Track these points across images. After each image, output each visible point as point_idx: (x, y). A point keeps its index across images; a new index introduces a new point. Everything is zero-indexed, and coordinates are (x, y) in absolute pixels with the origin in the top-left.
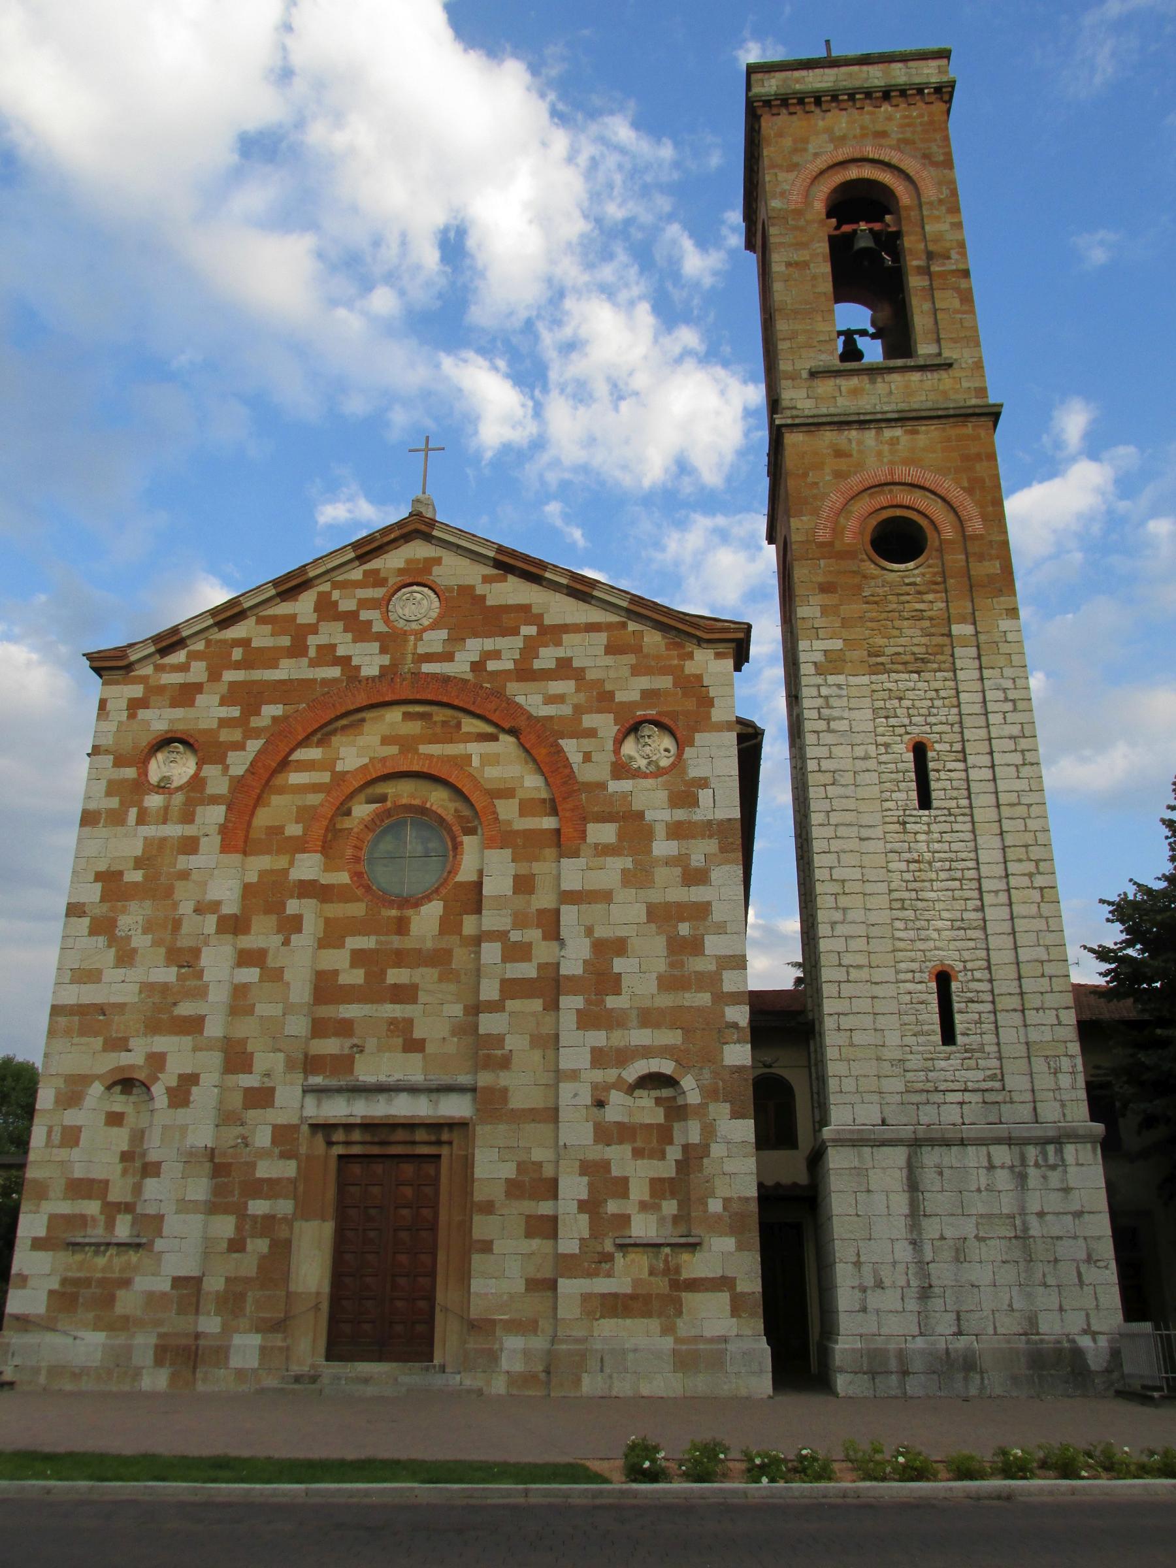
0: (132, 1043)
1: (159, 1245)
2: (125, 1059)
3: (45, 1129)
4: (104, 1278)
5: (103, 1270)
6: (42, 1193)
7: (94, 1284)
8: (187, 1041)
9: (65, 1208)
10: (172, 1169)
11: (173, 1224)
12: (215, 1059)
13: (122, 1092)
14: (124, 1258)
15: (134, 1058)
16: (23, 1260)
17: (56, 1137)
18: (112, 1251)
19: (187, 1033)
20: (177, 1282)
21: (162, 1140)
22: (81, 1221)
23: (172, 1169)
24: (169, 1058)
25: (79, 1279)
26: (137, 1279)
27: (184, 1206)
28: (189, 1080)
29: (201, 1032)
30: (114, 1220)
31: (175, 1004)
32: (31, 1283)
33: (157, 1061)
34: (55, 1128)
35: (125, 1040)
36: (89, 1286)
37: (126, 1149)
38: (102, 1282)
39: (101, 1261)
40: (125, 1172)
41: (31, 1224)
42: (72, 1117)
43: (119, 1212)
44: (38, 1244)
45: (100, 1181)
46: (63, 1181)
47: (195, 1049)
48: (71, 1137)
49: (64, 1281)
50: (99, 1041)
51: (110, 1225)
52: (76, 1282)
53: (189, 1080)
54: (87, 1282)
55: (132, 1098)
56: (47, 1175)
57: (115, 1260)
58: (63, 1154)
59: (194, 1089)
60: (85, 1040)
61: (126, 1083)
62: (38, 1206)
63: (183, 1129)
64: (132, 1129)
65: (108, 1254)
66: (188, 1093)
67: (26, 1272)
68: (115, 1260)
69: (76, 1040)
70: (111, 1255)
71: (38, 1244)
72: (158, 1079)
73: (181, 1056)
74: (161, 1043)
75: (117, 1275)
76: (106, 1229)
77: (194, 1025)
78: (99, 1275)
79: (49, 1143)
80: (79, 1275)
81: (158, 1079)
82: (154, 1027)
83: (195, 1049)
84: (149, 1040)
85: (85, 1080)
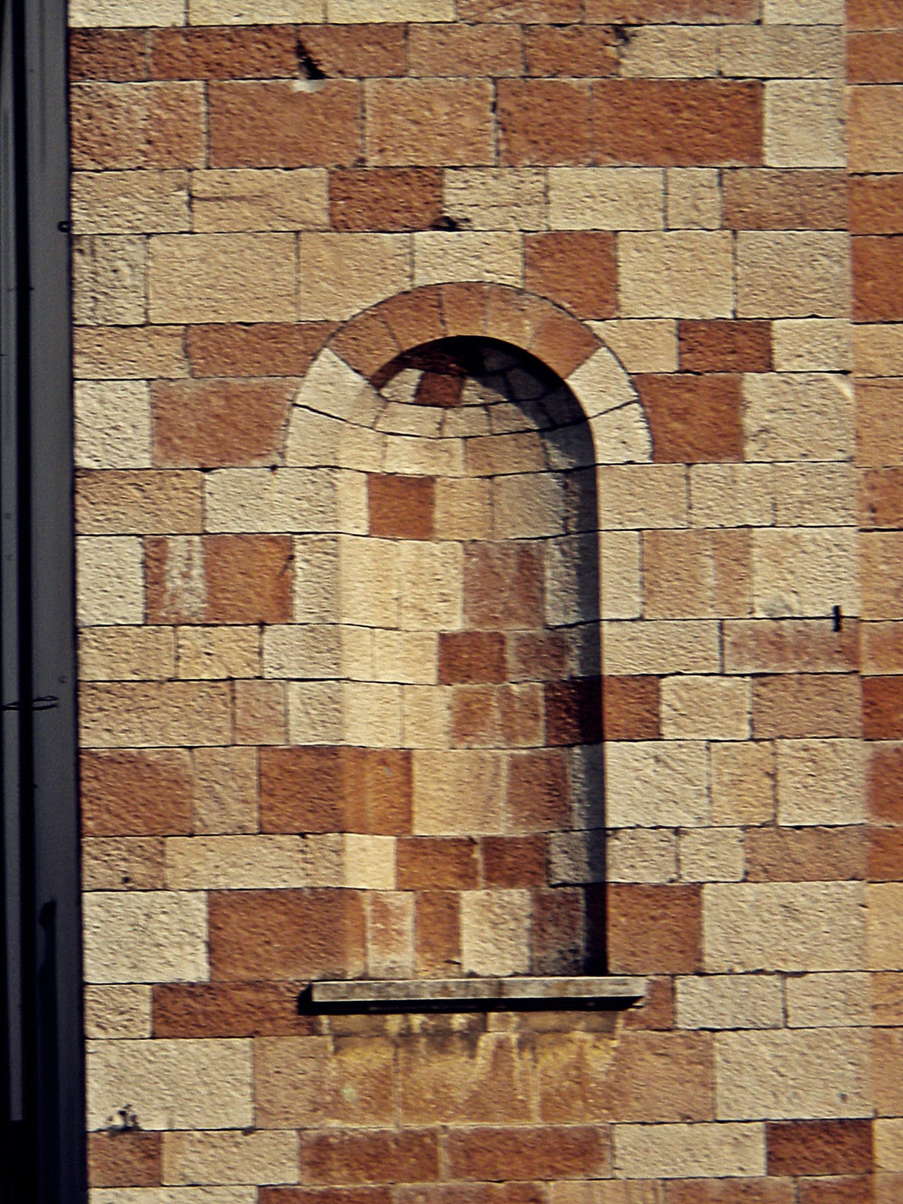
0: (457, 196)
1: (694, 1001)
2: (437, 260)
3: (132, 551)
4: (477, 1133)
5: (476, 1105)
6: (164, 808)
7: (444, 1158)
8: (696, 186)
9: (273, 866)
10: (706, 708)
11: (739, 917)
12: (824, 257)
13: (422, 397)
14: (555, 1059)
15: (475, 255)
16: (125, 1075)
17: (188, 585)
18: (502, 1029)
19: (678, 153)
20: (787, 1140)
21: (648, 591)
22: (327, 912)
23: (706, 708)
24: (630, 264)
25: (378, 1141)
26: (626, 1136)
27: (774, 852)
28: (728, 348)
29: (751, 148)
30: (453, 907)
31: (621, 33)
32: (174, 1161)
33: (580, 266)
34: (177, 546)
35: (430, 178)
36: (430, 1170)
37: (457, 624)
38: (472, 1152)
39: (464, 1071)
40: (466, 722)
41: (136, 937)
42: (241, 501)
43: (468, 879)
44: (178, 1011)
45: (383, 758)
46: (247, 761)
47: (735, 221)
48: (256, 581)
49: (318, 1153)
50: (308, 192)
51: (441, 930)
52: (372, 1154)
53: (728, 348)
54: (419, 1151)
55: (460, 421)
56: (177, 735)
57: (520, 1063)
58: (225, 650)
59: (754, 385)
60: (246, 179)
61: (453, 362)
62: (158, 860)
63: (734, 548)
64: (471, 547)
65: (486, 1042)
66: (734, 400)
67: (152, 1123)
68: (520, 1063)
69: (206, 181)
70: (501, 1045)
71: (178, 1011)
72: (595, 342)
73: (669, 255)
74: (585, 195)
75: (537, 1123)
76: (424, 945)
77: (716, 121)
78: (466, 1126)
79: (157, 611)
80: (372, 1126)
81: (595, 342)
82: (539, 131)
83: (735, 221)
84: (532, 182)
85: (290, 345)
